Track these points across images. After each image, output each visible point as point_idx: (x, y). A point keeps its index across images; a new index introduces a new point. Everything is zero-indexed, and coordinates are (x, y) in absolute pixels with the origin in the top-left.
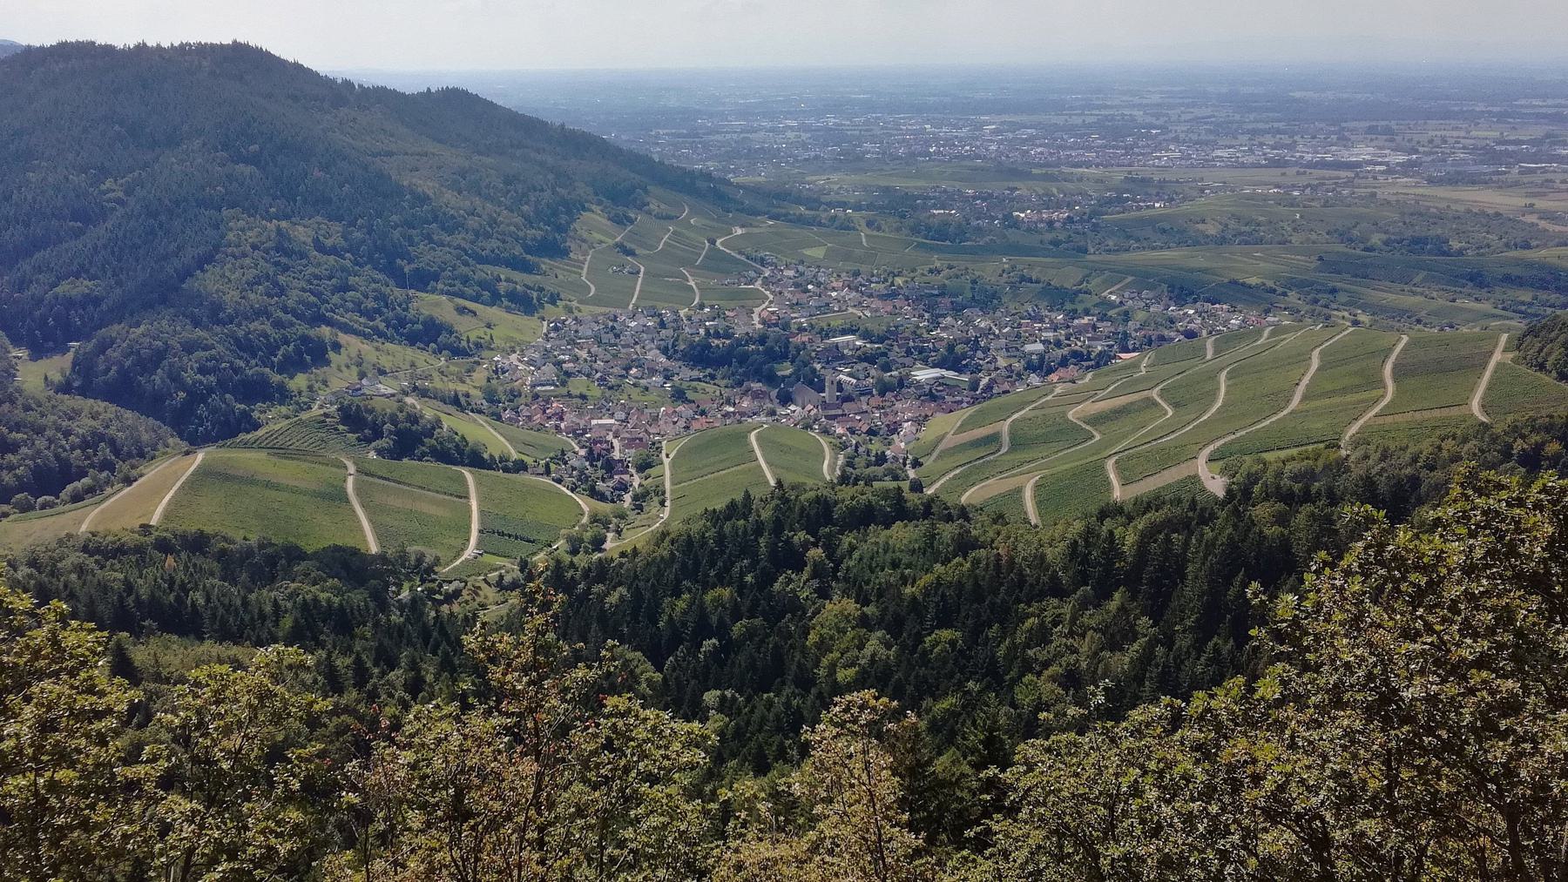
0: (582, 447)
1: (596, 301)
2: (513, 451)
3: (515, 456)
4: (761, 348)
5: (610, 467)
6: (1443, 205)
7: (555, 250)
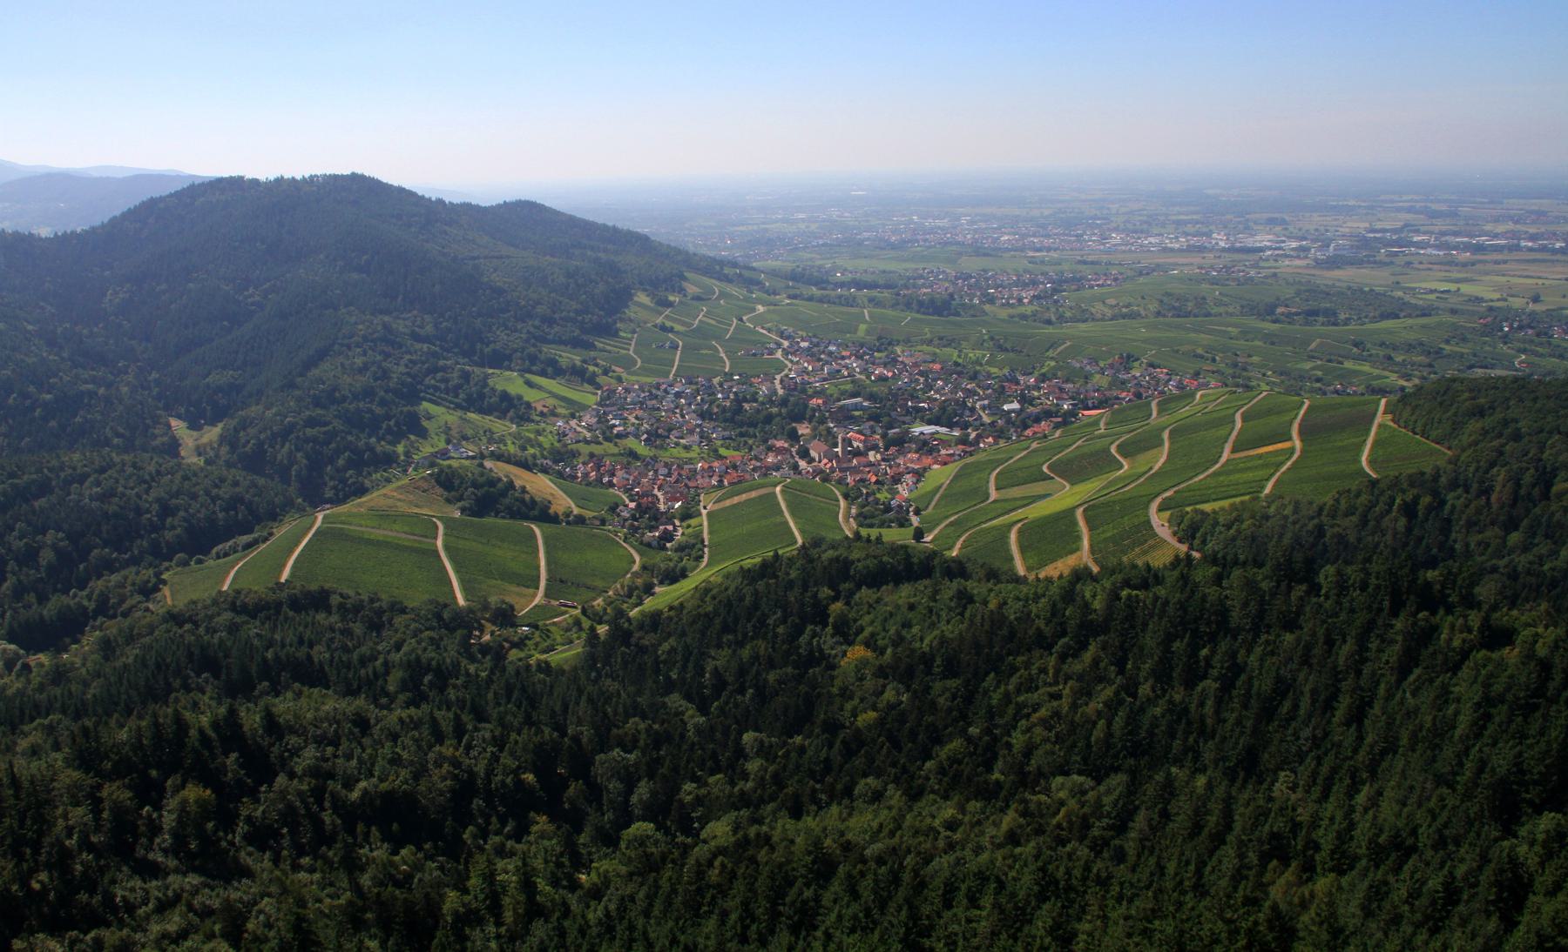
0: (632, 501)
1: (645, 371)
2: (573, 506)
3: (576, 511)
4: (784, 411)
5: (656, 518)
6: (1330, 283)
7: (609, 331)
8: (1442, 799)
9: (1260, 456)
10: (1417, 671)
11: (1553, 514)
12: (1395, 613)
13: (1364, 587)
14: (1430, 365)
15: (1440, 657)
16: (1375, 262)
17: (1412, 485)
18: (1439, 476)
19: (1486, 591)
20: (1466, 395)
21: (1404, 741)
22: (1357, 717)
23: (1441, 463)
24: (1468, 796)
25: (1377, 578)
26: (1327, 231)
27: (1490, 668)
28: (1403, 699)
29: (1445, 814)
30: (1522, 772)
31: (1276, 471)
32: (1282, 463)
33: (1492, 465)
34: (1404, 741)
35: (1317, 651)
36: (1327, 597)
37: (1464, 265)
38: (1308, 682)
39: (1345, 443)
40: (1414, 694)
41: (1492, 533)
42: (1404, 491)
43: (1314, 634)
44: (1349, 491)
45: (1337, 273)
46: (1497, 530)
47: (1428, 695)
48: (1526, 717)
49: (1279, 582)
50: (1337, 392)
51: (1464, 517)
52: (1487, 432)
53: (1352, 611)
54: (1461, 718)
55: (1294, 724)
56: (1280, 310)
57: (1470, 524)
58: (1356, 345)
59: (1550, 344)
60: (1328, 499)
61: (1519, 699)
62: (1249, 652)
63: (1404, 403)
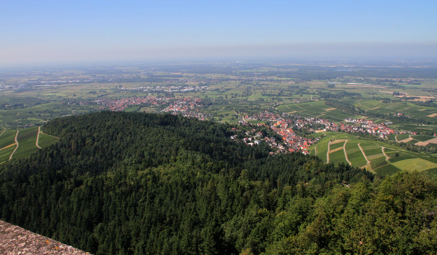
6: (20, 96)
8: (74, 229)
9: (7, 149)
10: (61, 198)
11: (87, 149)
12: (52, 184)
13: (42, 179)
14: (51, 116)
15: (66, 193)
16: (32, 90)
17: (51, 149)
18: (58, 145)
19: (73, 173)
20: (61, 122)
21: (61, 218)
22: (48, 215)
23: (57, 141)
24: (80, 226)
25: (45, 176)
26: (17, 82)
27: (78, 192)
28: (59, 206)
29: (75, 233)
30: (91, 216)
31: (12, 152)
32: (14, 150)
33: (70, 139)
34: (61, 218)
35: (33, 200)
36: (32, 185)
37: (56, 88)
38: (32, 210)
39: (31, 140)
40: (61, 204)
41: (74, 157)
42: (49, 151)
43: (31, 196)
44: (34, 154)
45: (22, 94)
46: (75, 156)
47: (65, 203)
48: (89, 202)
49: (18, 184)
50: (27, 127)
51: (66, 154)
52: (68, 131)
53: (40, 187)
54: (74, 207)
55: (30, 223)
56: (6, 106)
57: (68, 156)
58: (30, 113)
59: (80, 106)
60: (29, 157)
61: (87, 198)
62: (13, 206)
63: (45, 127)
